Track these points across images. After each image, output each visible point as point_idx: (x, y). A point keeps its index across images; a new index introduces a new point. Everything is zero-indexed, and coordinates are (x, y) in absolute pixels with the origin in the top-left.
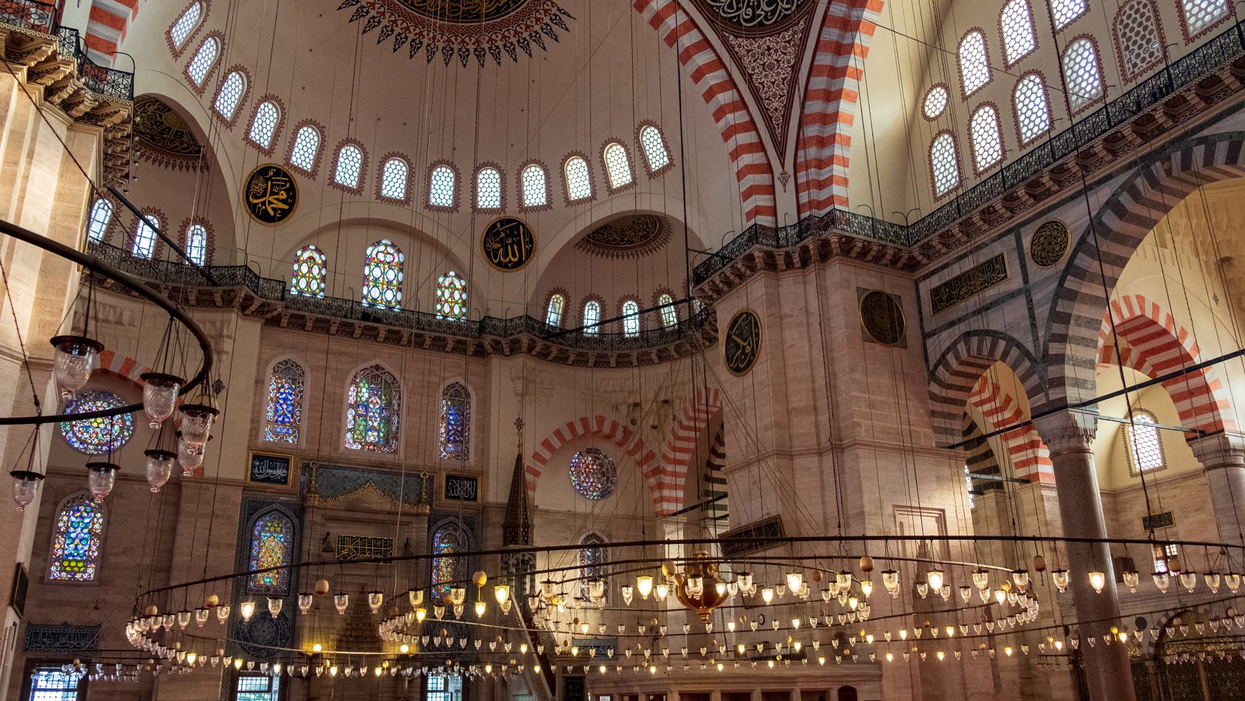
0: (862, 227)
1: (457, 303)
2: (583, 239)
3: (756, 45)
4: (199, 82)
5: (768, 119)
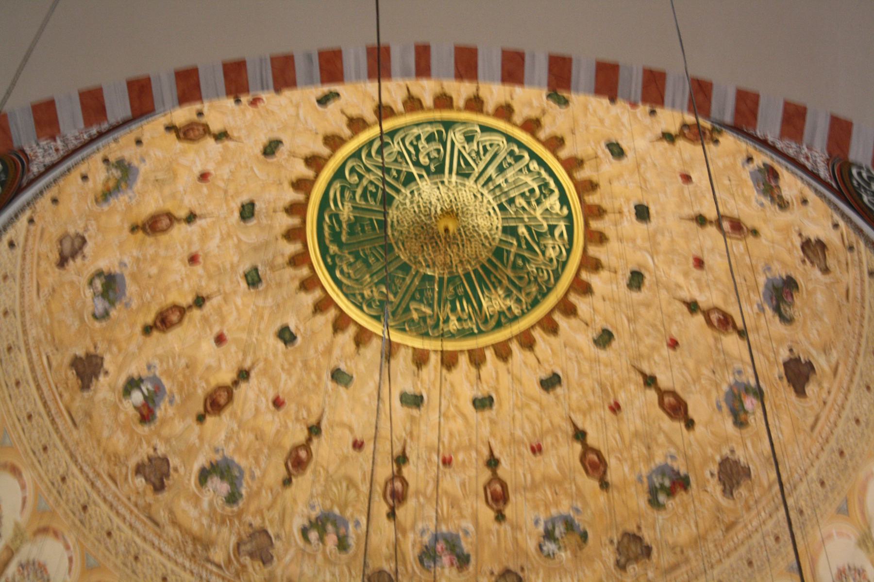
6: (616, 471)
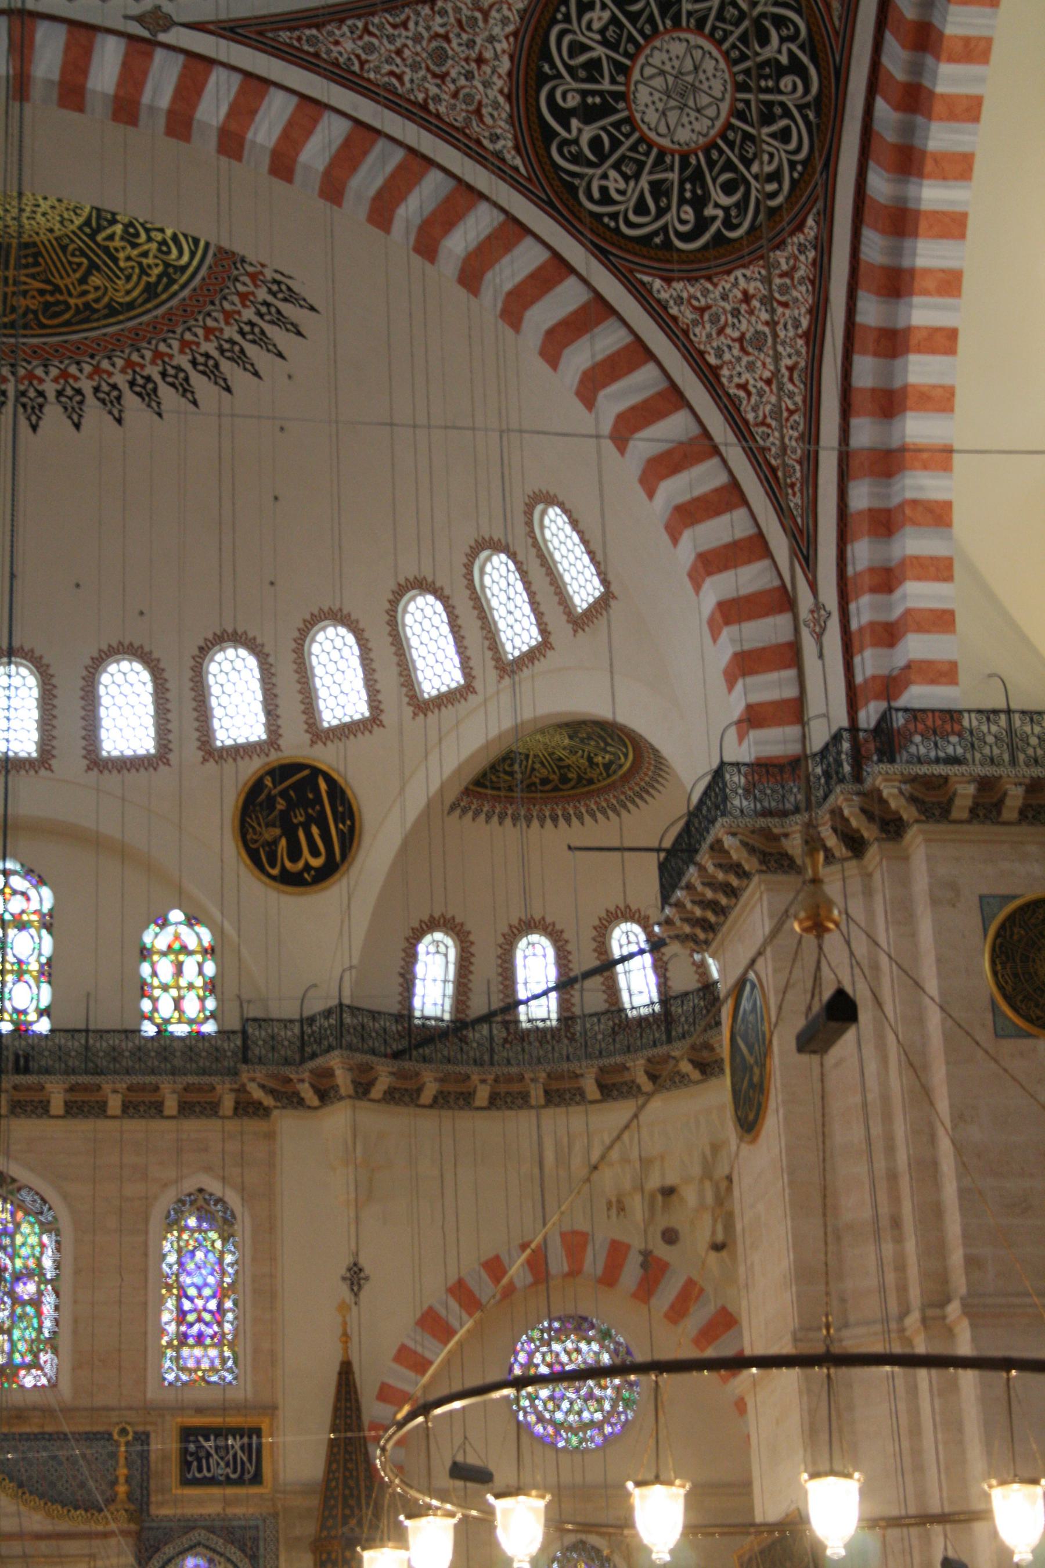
1: (191, 986)
2: (467, 792)
3: (717, 292)
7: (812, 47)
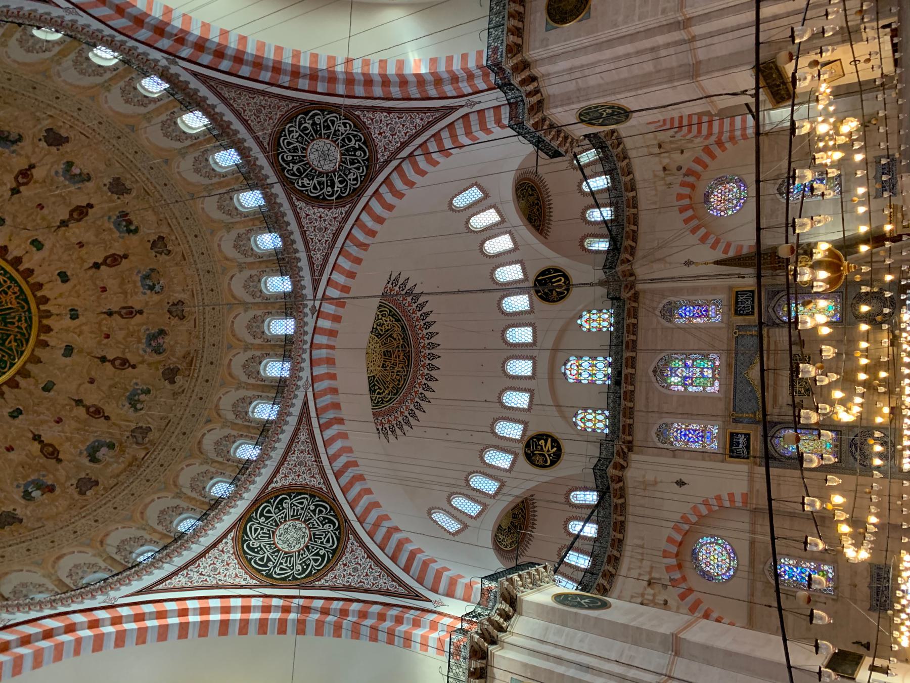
0: (496, 39)
1: (600, 317)
2: (541, 233)
4: (479, 508)
5: (431, 124)
6: (118, 249)
7: (306, 114)
